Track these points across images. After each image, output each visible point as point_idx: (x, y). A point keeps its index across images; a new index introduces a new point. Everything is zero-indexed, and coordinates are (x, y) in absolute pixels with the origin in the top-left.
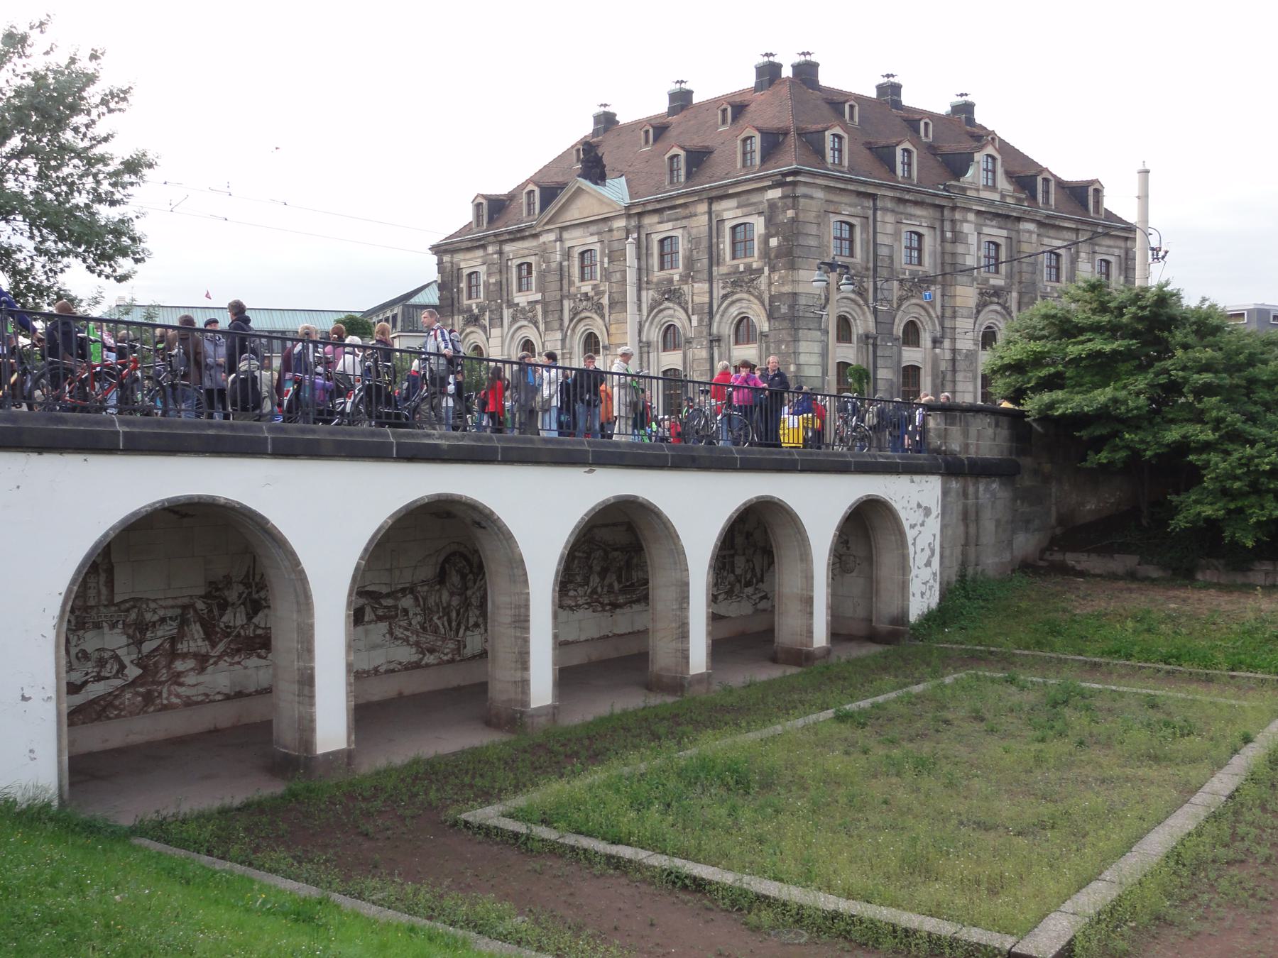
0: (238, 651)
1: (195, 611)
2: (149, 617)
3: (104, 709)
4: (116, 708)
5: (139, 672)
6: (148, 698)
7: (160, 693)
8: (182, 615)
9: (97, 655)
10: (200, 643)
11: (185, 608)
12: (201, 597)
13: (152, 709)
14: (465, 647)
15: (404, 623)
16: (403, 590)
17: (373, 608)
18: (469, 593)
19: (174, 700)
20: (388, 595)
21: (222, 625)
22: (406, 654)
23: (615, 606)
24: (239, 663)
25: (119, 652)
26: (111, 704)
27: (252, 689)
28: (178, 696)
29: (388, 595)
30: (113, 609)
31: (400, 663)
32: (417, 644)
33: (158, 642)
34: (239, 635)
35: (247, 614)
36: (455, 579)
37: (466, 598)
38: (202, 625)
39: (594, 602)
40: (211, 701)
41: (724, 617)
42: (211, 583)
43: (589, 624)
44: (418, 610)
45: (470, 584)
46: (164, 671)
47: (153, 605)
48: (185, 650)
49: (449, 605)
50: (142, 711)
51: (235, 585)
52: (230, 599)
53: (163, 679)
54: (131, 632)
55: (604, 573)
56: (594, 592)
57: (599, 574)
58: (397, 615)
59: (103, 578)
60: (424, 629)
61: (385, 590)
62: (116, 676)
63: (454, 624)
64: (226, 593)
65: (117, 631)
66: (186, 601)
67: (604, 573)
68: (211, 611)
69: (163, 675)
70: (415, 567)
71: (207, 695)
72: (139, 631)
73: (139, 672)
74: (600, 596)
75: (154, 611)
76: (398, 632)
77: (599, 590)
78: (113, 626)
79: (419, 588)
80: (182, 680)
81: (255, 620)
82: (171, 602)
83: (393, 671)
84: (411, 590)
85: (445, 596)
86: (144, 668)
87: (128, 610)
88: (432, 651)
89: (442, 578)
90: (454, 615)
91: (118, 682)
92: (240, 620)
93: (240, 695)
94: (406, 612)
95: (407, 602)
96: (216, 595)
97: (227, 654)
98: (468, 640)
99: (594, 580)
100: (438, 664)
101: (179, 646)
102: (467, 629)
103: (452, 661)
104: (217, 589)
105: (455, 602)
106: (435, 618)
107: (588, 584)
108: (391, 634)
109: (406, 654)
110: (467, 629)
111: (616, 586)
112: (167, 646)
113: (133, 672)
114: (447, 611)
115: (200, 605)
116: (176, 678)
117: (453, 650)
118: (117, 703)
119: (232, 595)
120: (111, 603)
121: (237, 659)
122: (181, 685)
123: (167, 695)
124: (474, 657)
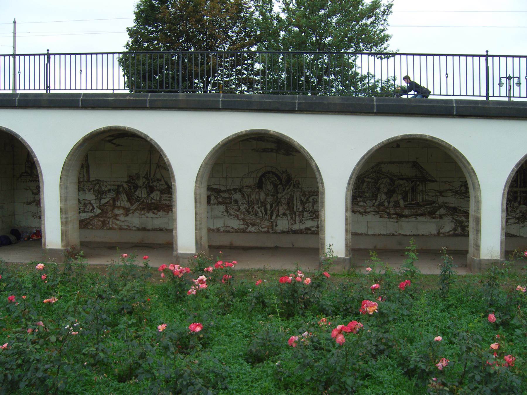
0: (144, 209)
1: (123, 188)
3: (87, 224)
4: (91, 225)
5: (100, 211)
6: (104, 223)
7: (109, 222)
9: (83, 202)
10: (125, 202)
11: (119, 186)
12: (126, 182)
13: (105, 228)
14: (276, 226)
15: (236, 208)
16: (235, 190)
17: (215, 197)
18: (279, 196)
19: (114, 226)
20: (225, 191)
21: (135, 196)
22: (235, 224)
23: (400, 216)
24: (144, 214)
25: (92, 202)
26: (89, 223)
27: (150, 227)
28: (116, 224)
29: (225, 191)
30: (89, 183)
31: (233, 228)
32: (244, 220)
33: (106, 200)
34: (143, 202)
35: (147, 192)
36: (270, 187)
37: (277, 198)
39: (381, 211)
40: (130, 230)
41: (514, 236)
42: (130, 176)
43: (377, 225)
45: (280, 191)
46: (110, 213)
47: (105, 184)
48: (119, 205)
49: (265, 200)
50: (101, 228)
52: (139, 185)
53: (110, 216)
54: (96, 194)
55: (390, 193)
56: (381, 204)
57: (386, 194)
58: (231, 203)
59: (85, 171)
61: (223, 188)
62: (90, 212)
64: (137, 182)
65: (91, 193)
66: (119, 183)
67: (390, 193)
68: (130, 189)
69: (110, 214)
70: (243, 178)
71: (129, 227)
72: (100, 194)
73: (100, 211)
74: (387, 208)
75: (106, 186)
76: (232, 212)
77: (386, 204)
78: (89, 191)
79: (245, 190)
80: (118, 218)
81: (152, 196)
82: (112, 183)
83: (228, 232)
84: (240, 190)
85: (262, 196)
86: (102, 210)
87: (95, 185)
88: (253, 225)
89: (260, 185)
90: (268, 207)
91: (92, 214)
92: (144, 195)
93: (144, 229)
94: (236, 202)
95: (237, 196)
97: (138, 210)
98: (279, 223)
99: (382, 197)
100: (258, 232)
101: (116, 203)
102: (278, 215)
103: (268, 232)
104: (133, 180)
105: (269, 199)
106: (256, 207)
108: (227, 212)
109: (235, 224)
110: (278, 215)
111: (402, 203)
112: (111, 202)
113: (98, 211)
114: (263, 204)
115: (125, 186)
116: (116, 217)
117: (268, 226)
118: (91, 223)
119: (141, 182)
120: (88, 181)
121: (143, 212)
122: (118, 220)
123: (111, 223)
124: (283, 232)
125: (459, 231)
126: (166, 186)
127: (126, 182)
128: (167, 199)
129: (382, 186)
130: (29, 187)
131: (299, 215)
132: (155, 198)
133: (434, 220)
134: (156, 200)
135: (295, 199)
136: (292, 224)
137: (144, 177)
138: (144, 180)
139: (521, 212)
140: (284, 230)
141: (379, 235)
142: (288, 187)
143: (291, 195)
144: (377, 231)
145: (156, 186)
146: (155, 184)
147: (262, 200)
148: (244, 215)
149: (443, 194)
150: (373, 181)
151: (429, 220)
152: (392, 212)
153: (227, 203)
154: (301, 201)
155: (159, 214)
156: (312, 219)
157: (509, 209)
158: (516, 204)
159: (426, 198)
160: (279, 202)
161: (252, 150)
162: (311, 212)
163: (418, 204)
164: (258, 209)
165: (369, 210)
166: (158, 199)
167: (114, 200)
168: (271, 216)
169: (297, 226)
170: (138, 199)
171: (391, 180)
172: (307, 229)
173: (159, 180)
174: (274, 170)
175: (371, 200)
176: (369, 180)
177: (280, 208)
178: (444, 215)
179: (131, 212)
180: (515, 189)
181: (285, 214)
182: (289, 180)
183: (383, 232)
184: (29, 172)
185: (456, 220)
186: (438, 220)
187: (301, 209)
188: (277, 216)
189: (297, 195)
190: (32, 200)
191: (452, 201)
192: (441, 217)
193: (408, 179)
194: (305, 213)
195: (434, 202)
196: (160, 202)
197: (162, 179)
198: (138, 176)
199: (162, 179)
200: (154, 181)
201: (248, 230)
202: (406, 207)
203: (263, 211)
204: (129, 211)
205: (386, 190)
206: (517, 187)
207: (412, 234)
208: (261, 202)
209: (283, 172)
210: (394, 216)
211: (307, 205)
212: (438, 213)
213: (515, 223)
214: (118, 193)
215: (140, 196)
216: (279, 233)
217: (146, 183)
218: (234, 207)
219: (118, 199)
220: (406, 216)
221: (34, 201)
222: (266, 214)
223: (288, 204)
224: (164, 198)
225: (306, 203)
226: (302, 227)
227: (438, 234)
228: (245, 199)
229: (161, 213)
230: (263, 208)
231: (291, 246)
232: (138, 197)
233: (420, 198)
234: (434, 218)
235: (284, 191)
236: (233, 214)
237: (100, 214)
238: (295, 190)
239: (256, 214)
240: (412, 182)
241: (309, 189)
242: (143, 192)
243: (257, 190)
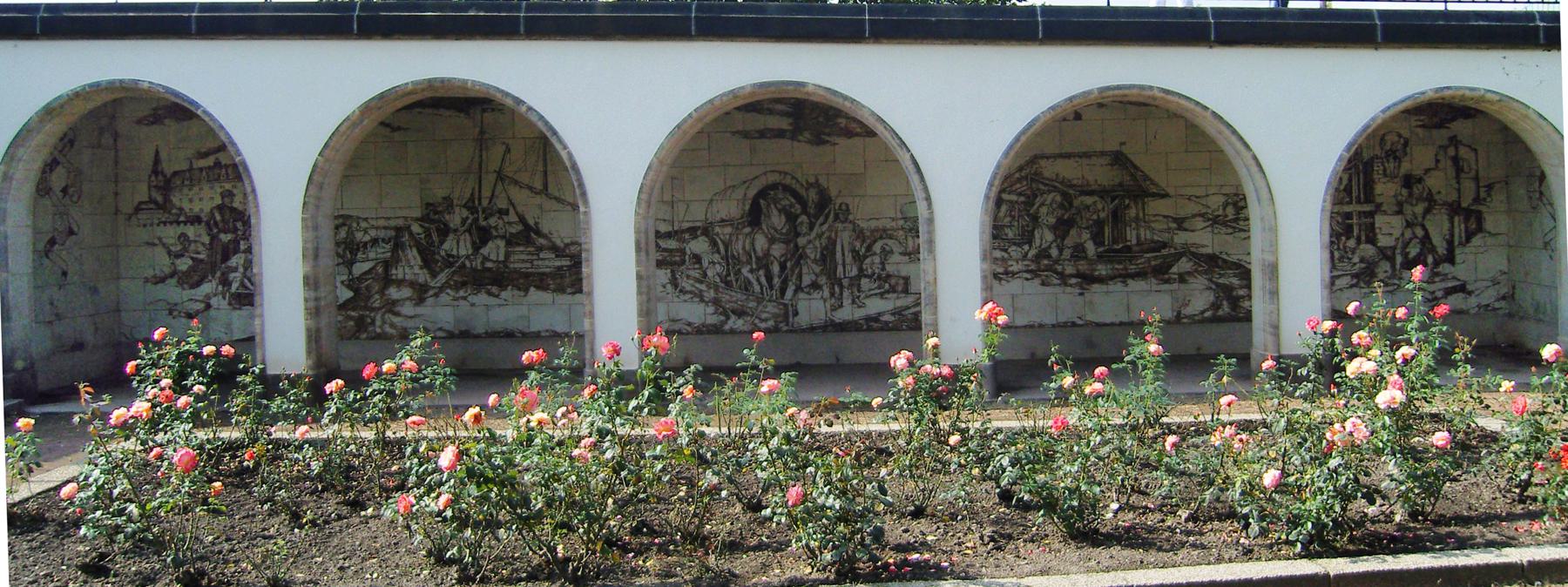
0: (464, 284)
1: (411, 234)
2: (359, 235)
5: (351, 294)
6: (361, 325)
8: (397, 237)
10: (417, 270)
11: (398, 229)
12: (417, 219)
14: (796, 314)
15: (696, 274)
16: (693, 231)
18: (801, 241)
19: (388, 329)
23: (1088, 279)
24: (465, 298)
27: (481, 330)
28: (392, 325)
31: (689, 324)
32: (716, 302)
33: (367, 266)
34: (464, 265)
35: (473, 243)
36: (778, 221)
38: (420, 252)
39: (1043, 269)
42: (428, 205)
44: (716, 258)
47: (364, 225)
48: (400, 276)
49: (767, 254)
51: (457, 210)
53: (376, 305)
55: (1062, 227)
56: (1043, 254)
57: (1053, 228)
58: (683, 262)
60: (728, 284)
63: (776, 281)
66: (400, 222)
68: (429, 235)
73: (350, 294)
74: (1057, 262)
75: (365, 231)
76: (686, 284)
77: (1054, 252)
79: (717, 229)
80: (398, 309)
81: (485, 251)
82: (382, 223)
84: (706, 231)
85: (761, 242)
86: (356, 291)
88: (740, 313)
89: (754, 217)
90: (776, 268)
92: (465, 249)
93: (465, 335)
94: (697, 259)
95: (699, 246)
97: (450, 287)
98: (802, 306)
102: (799, 289)
104: (436, 213)
105: (778, 250)
106: (745, 271)
107: (1030, 243)
108: (676, 286)
109: (697, 313)
110: (799, 289)
111: (1091, 248)
112: (380, 270)
114: (763, 262)
115: (416, 228)
116: (391, 306)
117: (775, 316)
119: (455, 219)
121: (462, 293)
122: (397, 314)
124: (812, 329)
125: (1226, 308)
128: (523, 257)
129: (1044, 210)
130: (160, 239)
131: (851, 285)
133: (1166, 286)
135: (838, 248)
136: (834, 309)
137: (465, 206)
138: (465, 213)
139: (1362, 261)
140: (816, 322)
141: (1041, 326)
142: (821, 219)
143: (829, 238)
144: (1036, 318)
145: (496, 228)
146: (492, 221)
147: (760, 254)
148: (717, 289)
149: (1186, 225)
150: (1022, 199)
151: (1155, 288)
152: (1070, 270)
153: (672, 264)
154: (855, 252)
155: (503, 294)
156: (881, 295)
157: (1336, 254)
158: (1351, 243)
159: (1145, 234)
160: (801, 257)
161: (734, 133)
162: (879, 278)
163: (1128, 249)
164: (750, 276)
165: (1015, 268)
166: (502, 258)
167: (387, 265)
168: (783, 291)
169: (847, 313)
170: (450, 261)
171: (1064, 195)
172: (868, 319)
173: (503, 213)
174: (788, 181)
175: (1019, 245)
176: (1014, 198)
177: (805, 270)
178: (1189, 273)
179: (431, 292)
180: (1347, 209)
181: (815, 286)
182: (824, 201)
183: (1049, 319)
184: (160, 199)
185: (1218, 285)
186: (1175, 286)
187: (855, 272)
188: (796, 291)
189: (845, 237)
190: (167, 270)
191: (1204, 239)
192: (1182, 279)
193: (1103, 193)
194: (864, 281)
195: (1164, 245)
197: (512, 211)
198: (448, 203)
200: (491, 215)
201: (727, 327)
202: (1100, 257)
203: (763, 280)
205: (1052, 220)
206: (1350, 202)
207: (1117, 320)
208: (758, 258)
209: (810, 185)
210: (1073, 281)
211: (868, 261)
212: (1174, 269)
213: (1352, 286)
214: (398, 246)
215: (455, 252)
216: (803, 331)
218: (692, 273)
219: (398, 261)
220: (1101, 280)
221: (172, 276)
222: (771, 287)
223: (823, 259)
225: (866, 257)
226: (859, 314)
227: (1179, 317)
228: (718, 252)
230: (761, 272)
231: (833, 361)
232: (449, 256)
233: (1131, 236)
234: (1167, 281)
235: (811, 229)
236: (688, 288)
237: (349, 301)
238: (840, 226)
239: (746, 287)
240: (1113, 200)
241: (873, 224)
243: (747, 230)
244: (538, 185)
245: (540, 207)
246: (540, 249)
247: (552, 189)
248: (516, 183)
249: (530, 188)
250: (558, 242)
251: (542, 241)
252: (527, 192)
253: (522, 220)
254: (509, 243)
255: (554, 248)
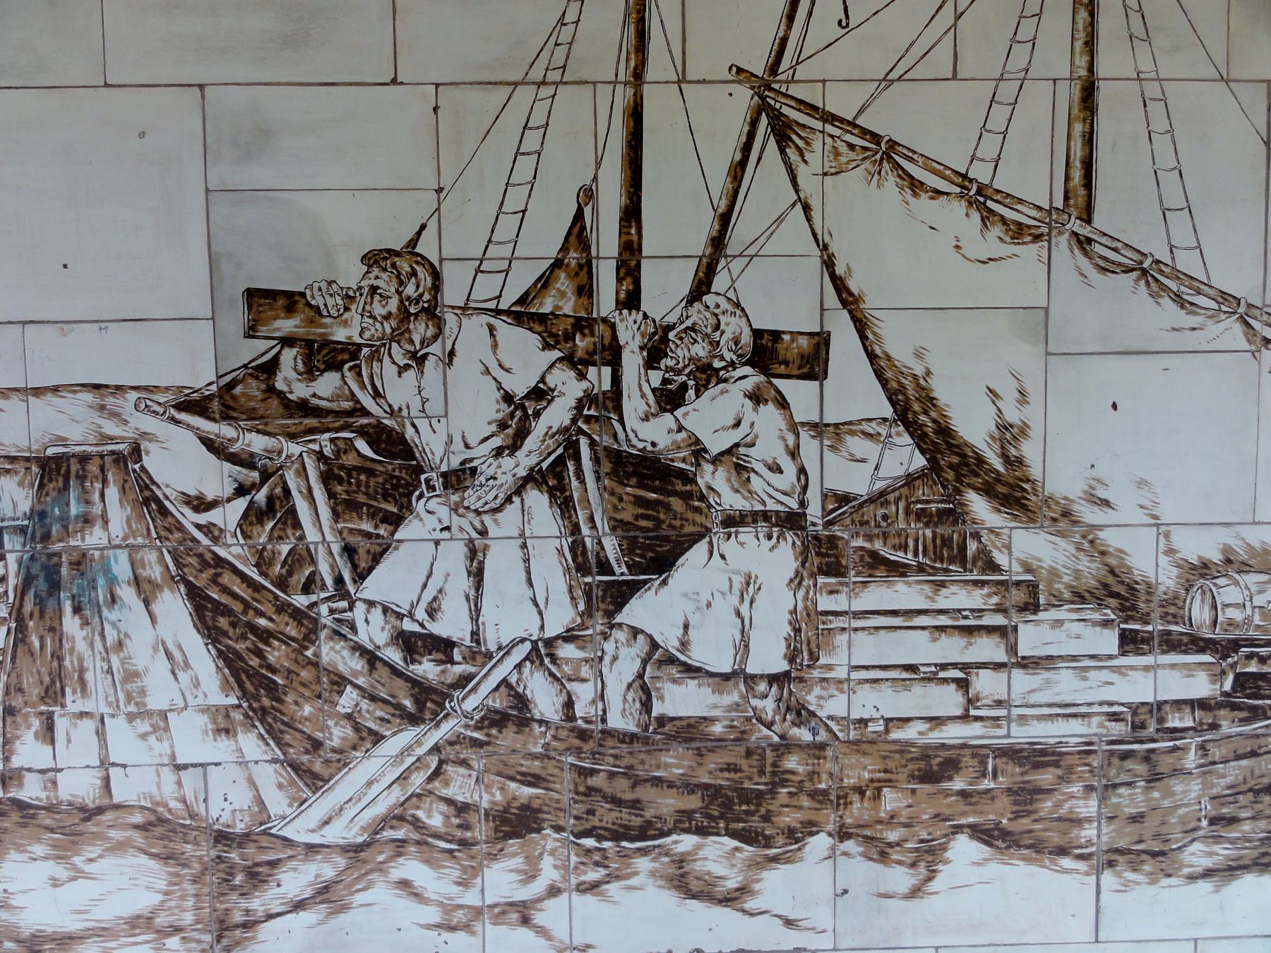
0: (516, 824)
1: (148, 499)
10: (191, 738)
12: (194, 405)
24: (523, 913)
34: (514, 713)
35: (582, 560)
38: (205, 611)
42: (261, 301)
48: (78, 785)
51: (470, 336)
52: (432, 443)
64: (400, 390)
66: (70, 425)
81: (655, 610)
96: (313, 396)
97: (424, 840)
104: (323, 355)
115: (182, 462)
119: (453, 403)
121: (500, 880)
126: (904, 457)
127: (194, 405)
132: (714, 652)
134: (737, 675)
137: (522, 315)
138: (526, 358)
145: (734, 460)
146: (713, 416)
155: (778, 886)
166: (768, 656)
179: (295, 880)
196: (802, 714)
197: (844, 345)
198: (411, 292)
199: (844, 345)
200: (706, 375)
204: (257, 877)
215: (452, 624)
217: (557, 415)
224: (869, 649)
229: (810, 880)
232: (411, 644)
242: (501, 561)
244: (1032, 178)
245: (1039, 321)
246: (1031, 598)
247: (1121, 212)
248: (885, 153)
249: (980, 198)
250: (1148, 563)
251: (1027, 547)
252: (955, 217)
253: (912, 408)
254: (823, 558)
255: (1117, 595)
